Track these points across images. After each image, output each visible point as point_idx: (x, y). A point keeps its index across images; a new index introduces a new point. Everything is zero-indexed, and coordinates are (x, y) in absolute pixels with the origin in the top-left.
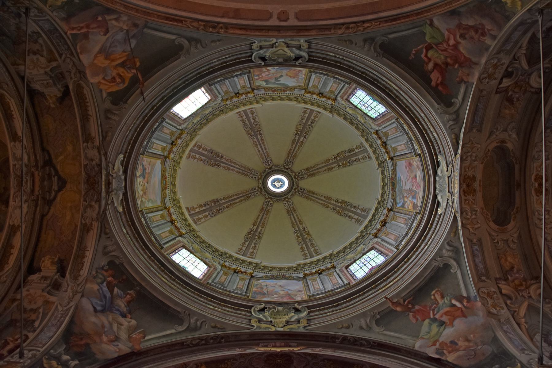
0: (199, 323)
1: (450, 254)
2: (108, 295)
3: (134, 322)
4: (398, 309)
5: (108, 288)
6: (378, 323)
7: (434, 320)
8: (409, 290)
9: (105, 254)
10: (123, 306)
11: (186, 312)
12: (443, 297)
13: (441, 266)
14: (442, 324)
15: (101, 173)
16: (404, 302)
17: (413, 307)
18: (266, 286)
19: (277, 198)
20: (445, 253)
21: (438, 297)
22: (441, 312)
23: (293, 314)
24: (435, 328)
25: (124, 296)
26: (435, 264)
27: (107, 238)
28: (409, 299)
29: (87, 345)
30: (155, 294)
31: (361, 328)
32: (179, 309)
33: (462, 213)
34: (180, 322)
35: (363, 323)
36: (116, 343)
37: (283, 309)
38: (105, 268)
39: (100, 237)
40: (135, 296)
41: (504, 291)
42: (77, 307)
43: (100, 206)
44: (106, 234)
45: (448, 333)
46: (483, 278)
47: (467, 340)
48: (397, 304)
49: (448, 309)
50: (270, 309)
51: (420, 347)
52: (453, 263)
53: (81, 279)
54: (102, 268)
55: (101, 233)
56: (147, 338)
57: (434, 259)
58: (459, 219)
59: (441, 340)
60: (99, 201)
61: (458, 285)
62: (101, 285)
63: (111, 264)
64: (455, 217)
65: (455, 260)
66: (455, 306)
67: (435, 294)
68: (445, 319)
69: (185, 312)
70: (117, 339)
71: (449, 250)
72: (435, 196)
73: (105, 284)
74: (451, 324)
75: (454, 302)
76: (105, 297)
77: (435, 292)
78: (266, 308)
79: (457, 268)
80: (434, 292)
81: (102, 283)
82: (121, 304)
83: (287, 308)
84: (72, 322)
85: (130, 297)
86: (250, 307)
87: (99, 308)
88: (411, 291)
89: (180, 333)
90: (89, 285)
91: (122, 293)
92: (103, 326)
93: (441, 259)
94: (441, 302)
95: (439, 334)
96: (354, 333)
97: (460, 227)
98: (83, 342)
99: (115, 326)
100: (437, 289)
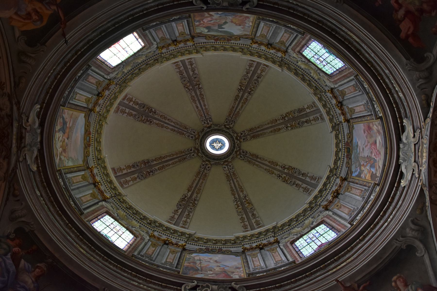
1: (415, 234)
2: (12, 268)
5: (13, 261)
8: (364, 274)
10: (30, 281)
11: (106, 289)
13: (404, 247)
15: (12, 125)
16: (359, 287)
18: (200, 260)
19: (215, 161)
20: (409, 233)
21: (400, 285)
25: (33, 269)
26: (397, 244)
27: (16, 201)
28: (364, 285)
30: (71, 268)
32: (97, 286)
33: (430, 187)
37: (218, 289)
38: (11, 237)
39: (7, 199)
40: (45, 269)
43: (9, 164)
44: (15, 196)
50: (203, 287)
52: (419, 245)
54: (8, 237)
55: (8, 194)
58: (427, 193)
60: (8, 157)
61: (426, 272)
62: (4, 257)
63: (19, 231)
64: (422, 190)
65: (421, 241)
69: (104, 289)
71: (414, 230)
72: (398, 166)
73: (9, 256)
76: (8, 271)
77: (397, 279)
78: (199, 286)
79: (424, 251)
80: (395, 278)
81: (6, 255)
83: (223, 288)
85: (39, 271)
86: (181, 285)
88: (366, 275)
91: (30, 266)
93: (404, 239)
97: (428, 203)
100: (398, 275)
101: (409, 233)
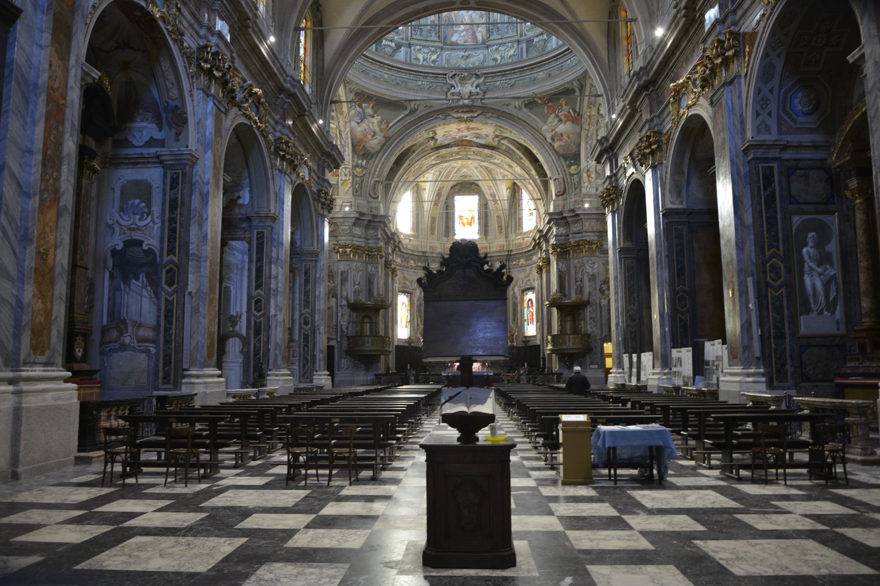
0: (416, 106)
2: (361, 110)
3: (379, 118)
4: (540, 101)
6: (526, 106)
7: (557, 116)
9: (351, 92)
12: (566, 105)
14: (560, 120)
17: (548, 103)
21: (564, 103)
22: (563, 113)
23: (474, 79)
24: (556, 120)
26: (567, 86)
29: (364, 146)
31: (515, 107)
34: (405, 108)
35: (517, 104)
36: (376, 137)
41: (601, 112)
42: (351, 131)
45: (562, 128)
46: (591, 106)
47: (568, 137)
48: (540, 98)
49: (566, 113)
51: (544, 131)
52: (577, 90)
53: (345, 114)
56: (390, 126)
57: (568, 83)
59: (557, 130)
63: (357, 94)
66: (570, 113)
67: (563, 101)
68: (563, 118)
70: (375, 133)
74: (565, 123)
75: (571, 111)
82: (369, 111)
84: (352, 139)
86: (446, 74)
87: (359, 121)
89: (406, 116)
90: (351, 114)
92: (365, 130)
94: (564, 107)
95: (557, 126)
96: (510, 110)
98: (361, 147)
99: (371, 125)
101: (575, 84)
